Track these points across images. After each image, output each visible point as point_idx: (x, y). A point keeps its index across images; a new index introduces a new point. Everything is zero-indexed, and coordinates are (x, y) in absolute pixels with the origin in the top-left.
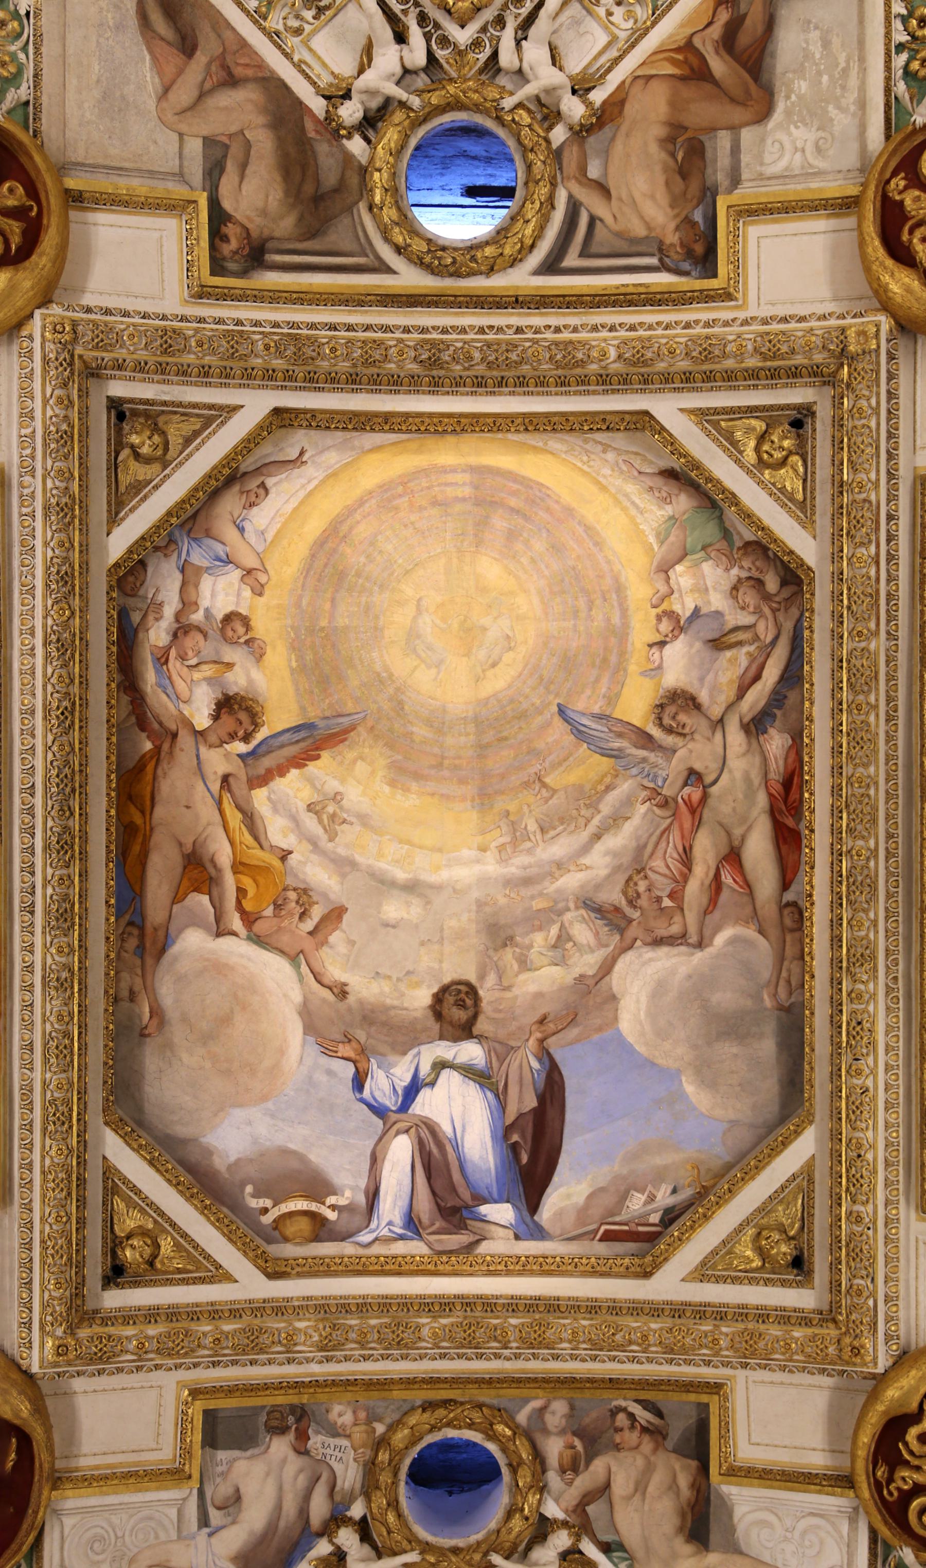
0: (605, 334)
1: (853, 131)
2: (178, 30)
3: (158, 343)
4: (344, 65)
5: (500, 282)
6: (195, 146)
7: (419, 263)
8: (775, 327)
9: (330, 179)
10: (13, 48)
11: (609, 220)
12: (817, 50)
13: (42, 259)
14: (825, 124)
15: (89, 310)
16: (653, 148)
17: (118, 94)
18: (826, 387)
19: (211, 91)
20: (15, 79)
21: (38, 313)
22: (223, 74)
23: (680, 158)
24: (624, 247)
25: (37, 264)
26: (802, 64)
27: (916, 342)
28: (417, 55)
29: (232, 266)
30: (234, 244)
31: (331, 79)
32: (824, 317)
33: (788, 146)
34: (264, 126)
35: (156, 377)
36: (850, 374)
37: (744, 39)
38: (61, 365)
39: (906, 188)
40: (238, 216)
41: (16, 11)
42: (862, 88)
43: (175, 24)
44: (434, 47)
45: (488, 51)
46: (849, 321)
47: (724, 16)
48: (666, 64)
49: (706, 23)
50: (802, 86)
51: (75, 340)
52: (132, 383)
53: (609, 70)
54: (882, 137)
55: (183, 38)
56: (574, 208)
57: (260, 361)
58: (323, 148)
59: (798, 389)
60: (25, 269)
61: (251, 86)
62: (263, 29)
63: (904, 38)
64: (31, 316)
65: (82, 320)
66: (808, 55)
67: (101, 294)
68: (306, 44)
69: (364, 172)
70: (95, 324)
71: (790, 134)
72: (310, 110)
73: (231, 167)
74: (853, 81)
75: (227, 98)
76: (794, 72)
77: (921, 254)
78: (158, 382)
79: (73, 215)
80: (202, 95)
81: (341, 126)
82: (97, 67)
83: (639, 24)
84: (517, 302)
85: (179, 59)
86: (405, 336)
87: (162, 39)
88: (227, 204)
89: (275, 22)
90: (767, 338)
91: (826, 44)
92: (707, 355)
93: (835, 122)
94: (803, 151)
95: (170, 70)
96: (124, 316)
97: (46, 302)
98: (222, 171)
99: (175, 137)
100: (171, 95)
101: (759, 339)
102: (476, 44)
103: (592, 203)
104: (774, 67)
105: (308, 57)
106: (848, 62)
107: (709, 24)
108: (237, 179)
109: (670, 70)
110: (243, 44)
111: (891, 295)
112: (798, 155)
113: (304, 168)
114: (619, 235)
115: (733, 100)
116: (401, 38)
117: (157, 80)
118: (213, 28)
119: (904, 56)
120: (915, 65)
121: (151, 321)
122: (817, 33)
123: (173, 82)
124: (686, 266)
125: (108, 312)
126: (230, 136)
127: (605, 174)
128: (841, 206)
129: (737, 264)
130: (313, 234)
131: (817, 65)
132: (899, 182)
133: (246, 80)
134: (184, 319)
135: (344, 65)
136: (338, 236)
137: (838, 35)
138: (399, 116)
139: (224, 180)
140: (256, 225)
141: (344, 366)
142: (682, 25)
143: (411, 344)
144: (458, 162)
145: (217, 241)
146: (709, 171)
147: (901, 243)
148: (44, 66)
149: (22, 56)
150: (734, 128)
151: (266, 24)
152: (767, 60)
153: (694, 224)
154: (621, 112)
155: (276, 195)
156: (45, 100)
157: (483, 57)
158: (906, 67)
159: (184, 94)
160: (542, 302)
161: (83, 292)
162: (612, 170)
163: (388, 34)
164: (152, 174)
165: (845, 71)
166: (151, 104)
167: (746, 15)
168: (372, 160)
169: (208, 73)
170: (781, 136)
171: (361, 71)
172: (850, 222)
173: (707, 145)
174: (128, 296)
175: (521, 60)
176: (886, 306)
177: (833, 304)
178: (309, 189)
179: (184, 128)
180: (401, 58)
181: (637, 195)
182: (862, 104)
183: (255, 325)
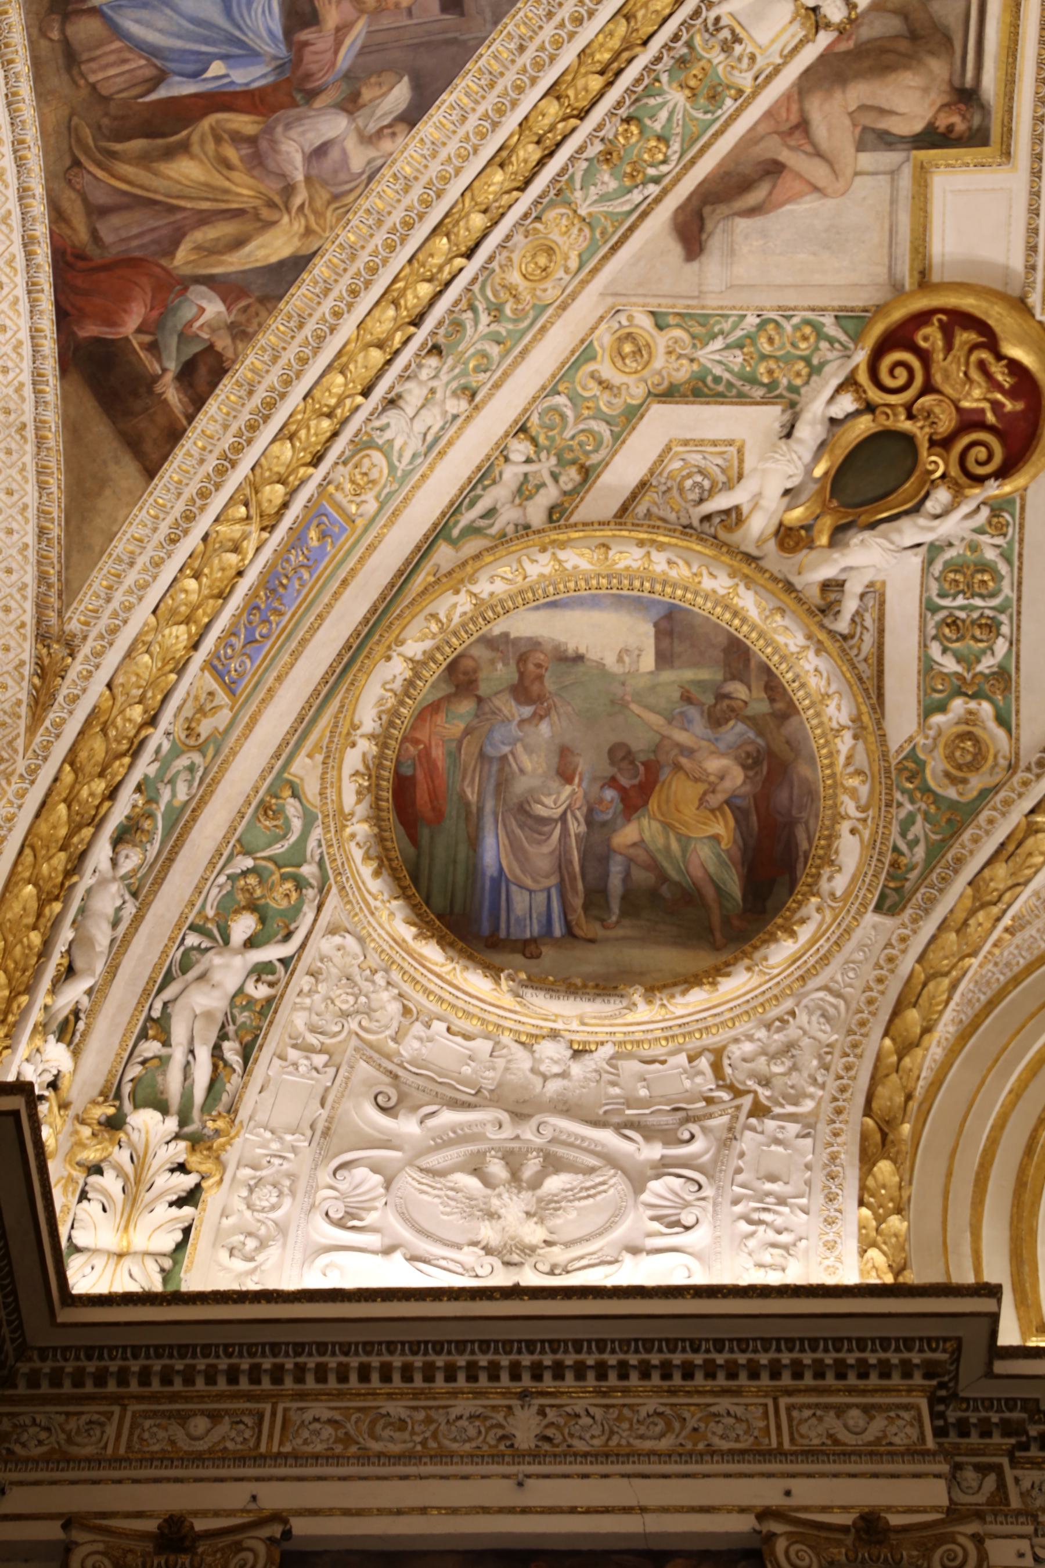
6: (867, 160)
19: (814, 145)
20: (817, 329)
22: (798, 134)
29: (977, 121)
30: (956, 119)
40: (929, 116)
58: (865, 33)
61: (807, 106)
62: (755, 94)
72: (830, 47)
73: (883, 124)
75: (820, 130)
79: (936, 277)
80: (819, 154)
81: (849, 18)
85: (786, 176)
87: (770, 193)
88: (918, 127)
89: (745, 81)
95: (798, 186)
98: (887, 133)
99: (858, 180)
100: (821, 184)
105: (777, 47)
108: (894, 118)
110: (769, 114)
113: (884, 51)
117: (808, 198)
126: (855, 125)
130: (948, 40)
133: (802, 111)
140: (938, 97)
145: (953, 136)
148: (806, 304)
149: (795, 320)
151: (748, 91)
155: (909, 79)
156: (836, 304)
159: (817, 171)
164: (893, 201)
166: (830, 203)
178: (903, 46)
179: (849, 171)
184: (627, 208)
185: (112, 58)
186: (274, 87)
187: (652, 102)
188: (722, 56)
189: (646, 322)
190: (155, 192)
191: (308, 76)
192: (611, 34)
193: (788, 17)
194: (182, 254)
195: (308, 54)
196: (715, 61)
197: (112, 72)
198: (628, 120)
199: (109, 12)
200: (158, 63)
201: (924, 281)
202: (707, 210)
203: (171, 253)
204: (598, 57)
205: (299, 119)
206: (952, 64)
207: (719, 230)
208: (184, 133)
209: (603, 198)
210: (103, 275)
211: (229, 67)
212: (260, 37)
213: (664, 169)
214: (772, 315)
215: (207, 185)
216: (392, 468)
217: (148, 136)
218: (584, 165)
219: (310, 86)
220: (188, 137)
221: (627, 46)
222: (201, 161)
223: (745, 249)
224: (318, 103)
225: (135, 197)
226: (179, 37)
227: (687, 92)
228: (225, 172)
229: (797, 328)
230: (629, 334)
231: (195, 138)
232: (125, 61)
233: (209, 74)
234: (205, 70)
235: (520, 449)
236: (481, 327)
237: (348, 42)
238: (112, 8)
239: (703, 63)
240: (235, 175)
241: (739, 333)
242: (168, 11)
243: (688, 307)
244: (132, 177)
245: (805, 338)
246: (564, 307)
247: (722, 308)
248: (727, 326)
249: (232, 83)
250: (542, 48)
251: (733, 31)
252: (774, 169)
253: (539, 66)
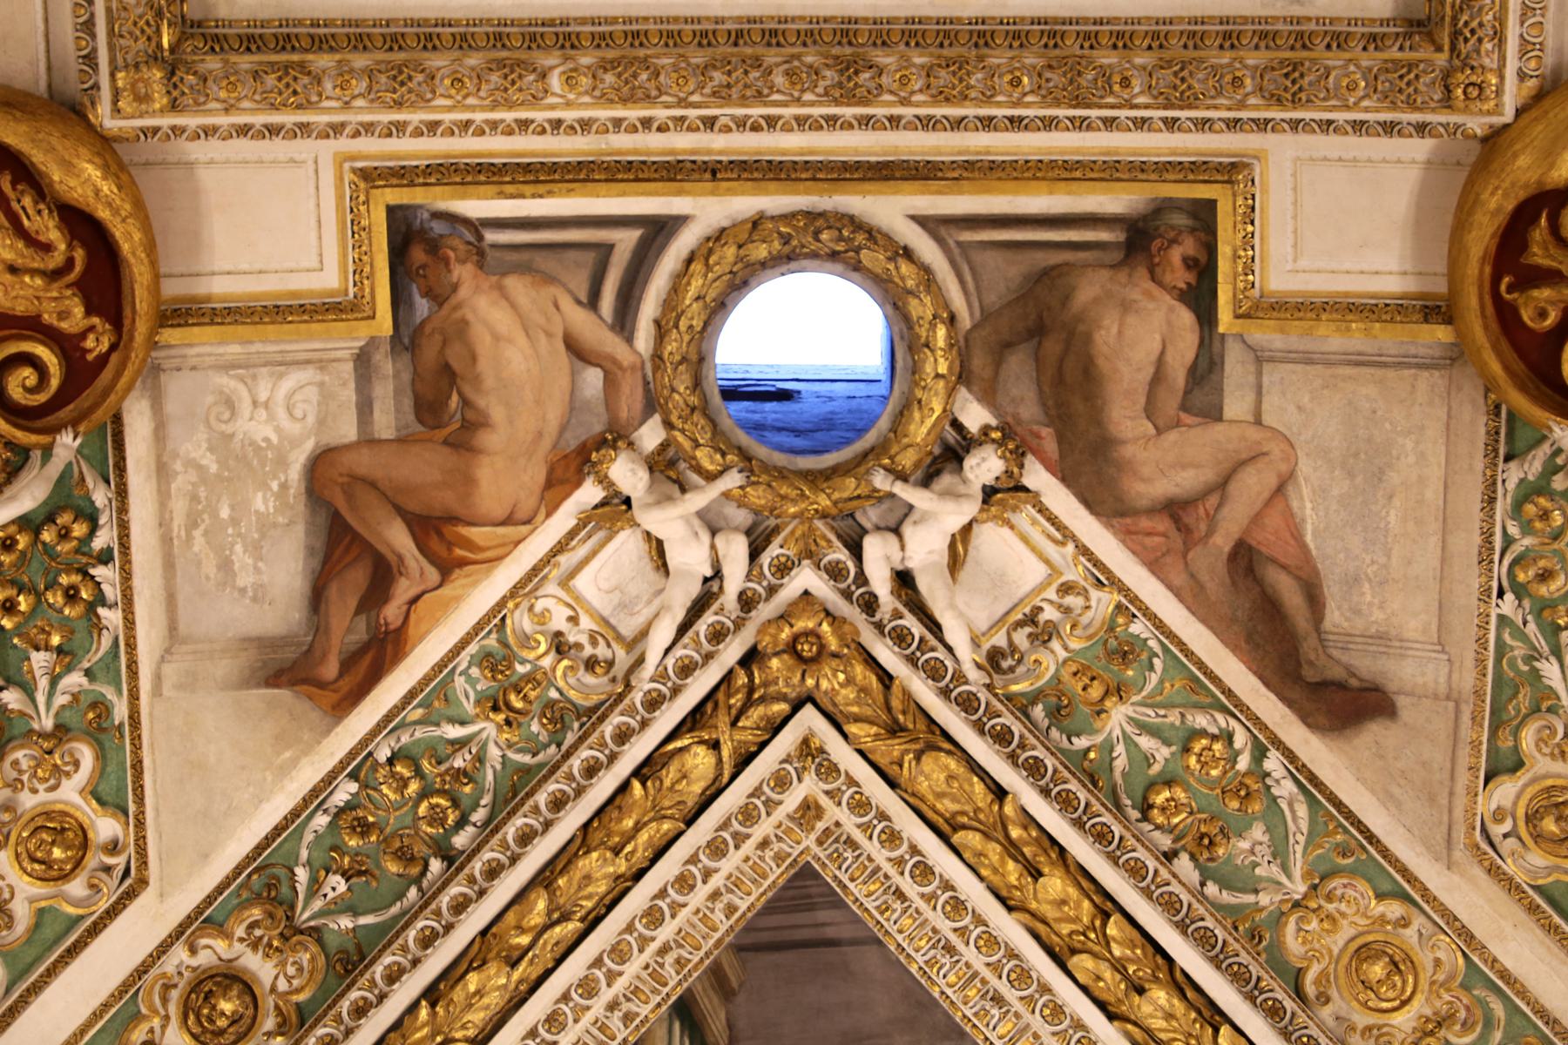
0: (569, 115)
1: (175, 430)
2: (1259, 582)
3: (1307, 80)
4: (993, 541)
5: (743, 204)
6: (1236, 405)
7: (873, 234)
8: (288, 118)
9: (1018, 365)
10: (1527, 541)
11: (567, 303)
12: (241, 556)
13: (1497, 202)
14: (222, 443)
15: (1421, 129)
16: (497, 413)
17: (1359, 479)
18: (197, 16)
20: (1529, 492)
21: (1508, 115)
22: (1188, 519)
23: (455, 398)
24: (542, 261)
25: (1506, 195)
26: (263, 536)
27: (50, 86)
28: (879, 556)
29: (1180, 220)
30: (1176, 255)
31: (1016, 519)
32: (209, 132)
33: (281, 412)
34: (1123, 442)
35: (1312, 26)
36: (158, 32)
37: (358, 577)
38: (1473, 32)
39: (83, 335)
40: (1168, 300)
41: (1519, 597)
42: (163, 497)
43: (1264, 593)
44: (851, 565)
45: (766, 559)
46: (166, 122)
47: (392, 612)
48: (481, 543)
49: (420, 603)
51: (1447, 75)
52: (1353, 14)
53: (572, 534)
54: (128, 419)
55: (1250, 571)
56: (624, 321)
57: (1138, 61)
58: (1029, 410)
59: (244, 16)
60: (1526, 186)
61: (1144, 503)
62: (1123, 589)
63: (99, 572)
64: (1519, 112)
65: (1433, 110)
66: (255, 549)
67: (1399, 161)
68: (1054, 570)
69: (963, 376)
70: (1412, 105)
71: (278, 429)
73: (1178, 375)
74: (179, 507)
75: (1183, 482)
76: (275, 525)
77: (51, 224)
78: (1309, 19)
79: (1440, 286)
80: (1222, 485)
81: (999, 444)
82: (1392, 518)
83: (525, 604)
84: (714, 172)
85: (1259, 539)
86: (898, 111)
87: (1284, 567)
88: (1185, 318)
89: (1103, 602)
90: (301, 99)
91: (226, 565)
92: (399, 76)
93: (205, 445)
94: (255, 403)
95: (1273, 520)
96: (1363, 123)
97: (1493, 140)
98: (1193, 370)
99: (1267, 419)
100: (1272, 481)
101: (314, 98)
102: (784, 569)
103: (594, 330)
104: (308, 533)
105: (1051, 550)
106: (189, 538)
107: (414, 601)
108: (1169, 358)
109: (475, 533)
110: (1154, 565)
111: (97, 160)
112: (263, 396)
113: (1059, 380)
114: (550, 279)
115: (373, 485)
117: (1295, 504)
118: (1202, 587)
119: (98, 543)
120: (79, 530)
121: (1318, 115)
122: (240, 583)
123: (1269, 503)
124: (438, 228)
125: (1389, 128)
126: (1178, 424)
127: (574, 374)
128: (188, 312)
129: (356, 228)
130: (1046, 276)
131: (239, 535)
132: (96, 345)
133: (1151, 511)
134: (1262, 125)
135: (993, 541)
136: (1005, 274)
137: (208, 578)
138: (907, 460)
139: (1190, 355)
140: (1138, 287)
141: (998, 58)
142: (458, 599)
143: (887, 97)
144: (808, 426)
145: (1203, 259)
146: (406, 377)
147: (84, 245)
149: (1513, 530)
150: (368, 441)
152: (319, 544)
153: (428, 293)
154: (551, 471)
155: (1106, 335)
156: (1479, 463)
157: (773, 551)
158: (94, 527)
159: (1252, 486)
160: (673, 172)
161: (1429, 162)
162: (564, 381)
163: (923, 584)
164: (1307, 359)
165: (192, 524)
166: (1305, 467)
167: (358, 612)
168: (951, 393)
169: (1212, 521)
170: (294, 428)
171: (967, 529)
172: (172, 289)
173: (411, 417)
174: (1355, 160)
175: (713, 547)
176: (105, 146)
177: (193, 157)
178: (1052, 346)
179: (1253, 434)
180: (903, 548)
181: (521, 340)
182: (162, 471)
183: (1144, 120)
184: (1302, 810)
187: (1120, 763)
188: (1055, 644)
189: (1506, 791)
192: (980, 854)
193: (1005, 532)
196: (1062, 654)
198: (1146, 809)
201: (1435, 310)
202: (1309, 675)
204: (1013, 879)
206: (1086, 266)
207: (1345, 658)
209: (1280, 853)
213: (1240, 739)
214: (1501, 569)
218: (1211, 889)
221: (996, 830)
223: (1378, 615)
227: (1108, 704)
229: (1527, 529)
230: (1528, 819)
239: (1066, 675)
241: (1532, 628)
243: (1476, 720)
245: (1545, 515)
246: (1469, 937)
247: (1480, 662)
248: (1519, 650)
250: (996, 968)
251: (1020, 624)
252: (1244, 559)
253: (1022, 975)
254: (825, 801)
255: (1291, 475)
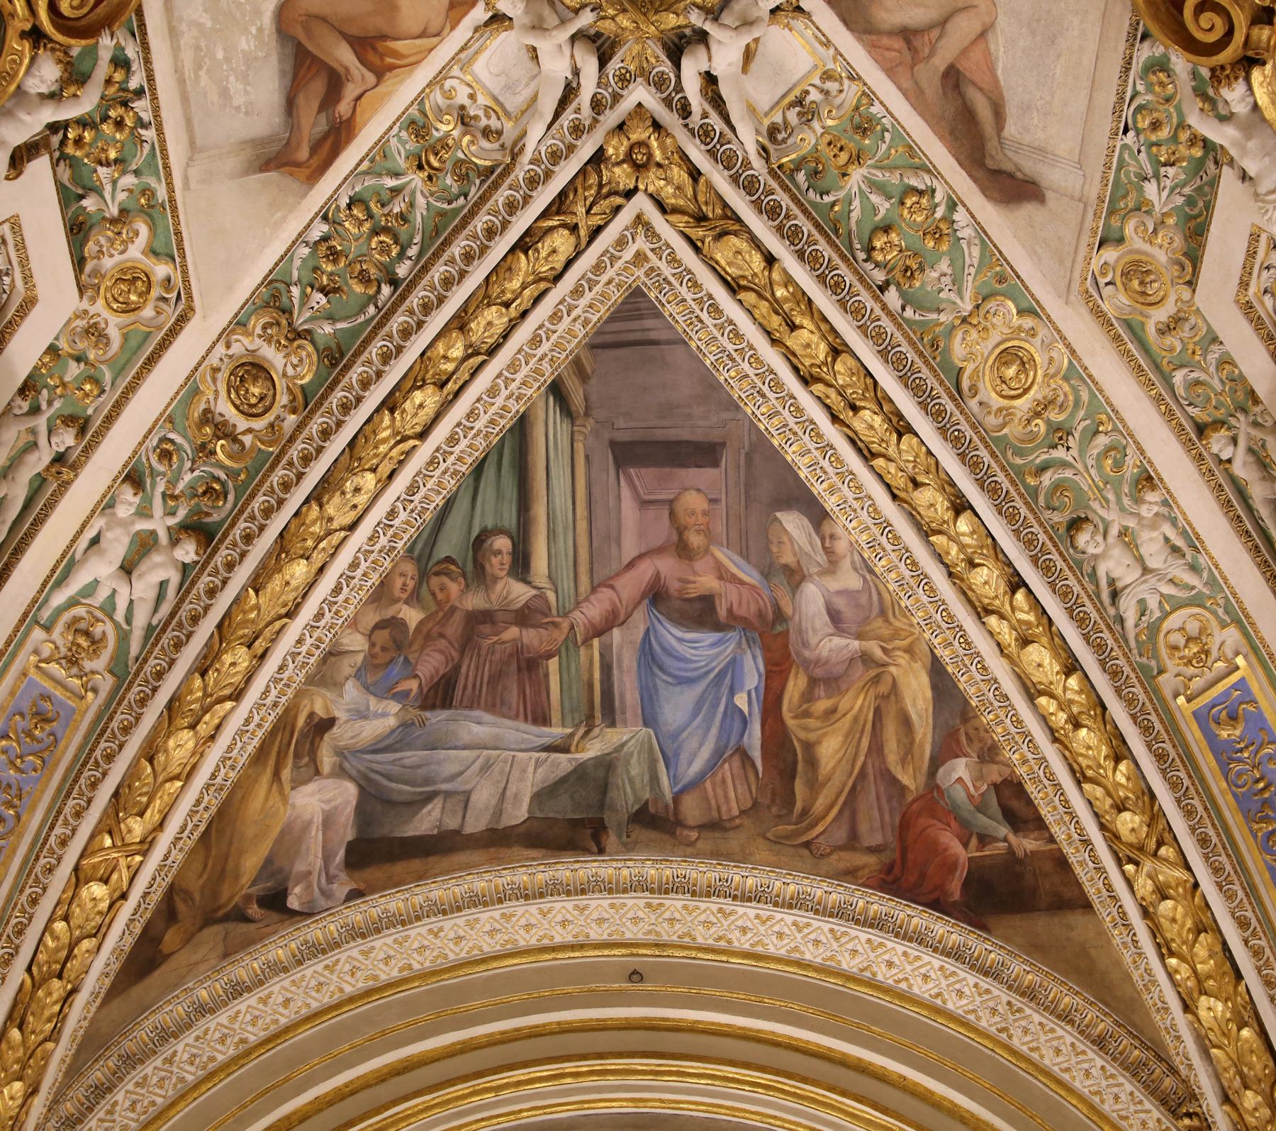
12: (234, 85)
17: (1039, 39)
26: (248, 68)
44: (672, 76)
50: (245, 44)
66: (244, 78)
76: (256, 59)
82: (1058, 71)
91: (225, 93)
93: (201, 8)
106: (197, 77)
116: (710, 79)
117: (992, 47)
119: (133, 84)
122: (235, 103)
131: (232, 69)
157: (614, 65)
166: (1002, 22)
180: (710, 60)
185: (720, 791)
186: (766, 649)
190: (844, 785)
191: (760, 614)
194: (906, 779)
195: (741, 611)
197: (732, 794)
199: (680, 786)
200: (729, 752)
203: (903, 789)
205: (800, 631)
208: (796, 743)
210: (910, 857)
211: (742, 689)
212: (718, 655)
214: (1128, 113)
215: (847, 735)
216: (1197, 601)
217: (793, 777)
219: (770, 616)
220: (800, 740)
222: (825, 735)
224: (788, 610)
225: (845, 804)
226: (708, 729)
228: (837, 716)
231: (802, 735)
232: (724, 781)
233: (745, 709)
234: (741, 711)
235: (1218, 444)
236: (1070, 459)
237: (734, 570)
238: (676, 784)
240: (843, 706)
241: (1143, 156)
242: (685, 735)
244: (828, 801)
249: (756, 688)
254: (650, 254)
255: (992, 25)
